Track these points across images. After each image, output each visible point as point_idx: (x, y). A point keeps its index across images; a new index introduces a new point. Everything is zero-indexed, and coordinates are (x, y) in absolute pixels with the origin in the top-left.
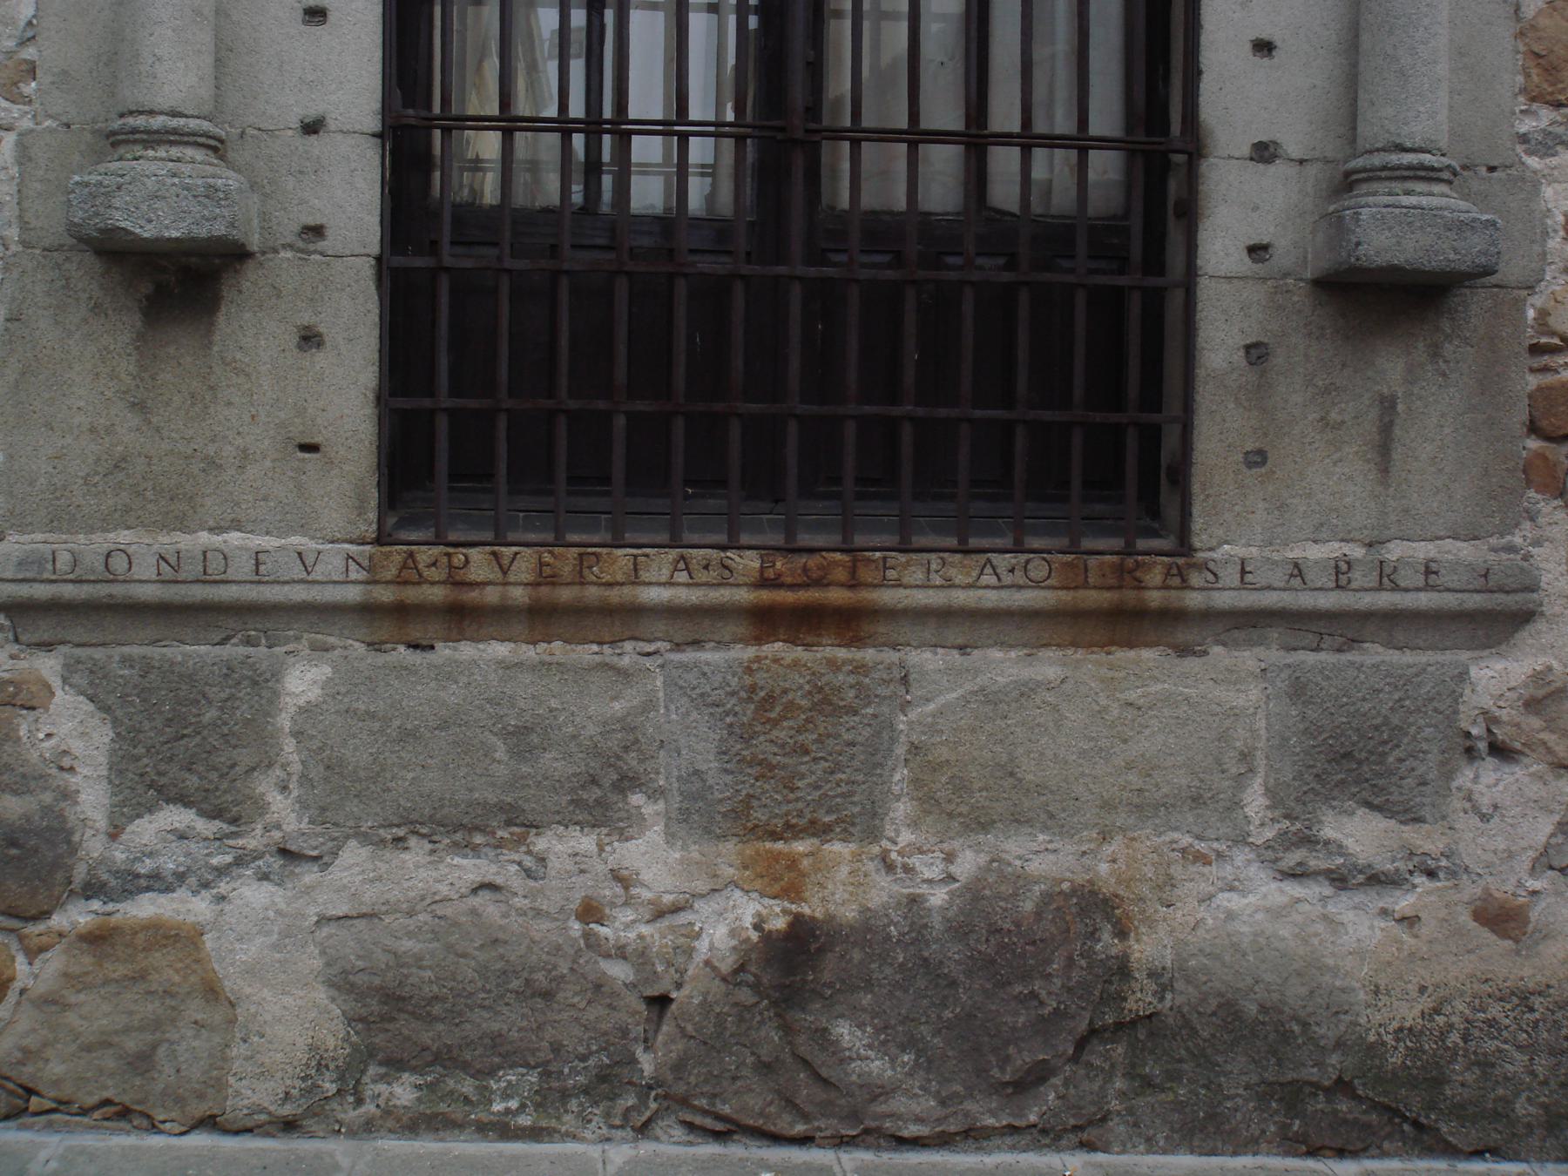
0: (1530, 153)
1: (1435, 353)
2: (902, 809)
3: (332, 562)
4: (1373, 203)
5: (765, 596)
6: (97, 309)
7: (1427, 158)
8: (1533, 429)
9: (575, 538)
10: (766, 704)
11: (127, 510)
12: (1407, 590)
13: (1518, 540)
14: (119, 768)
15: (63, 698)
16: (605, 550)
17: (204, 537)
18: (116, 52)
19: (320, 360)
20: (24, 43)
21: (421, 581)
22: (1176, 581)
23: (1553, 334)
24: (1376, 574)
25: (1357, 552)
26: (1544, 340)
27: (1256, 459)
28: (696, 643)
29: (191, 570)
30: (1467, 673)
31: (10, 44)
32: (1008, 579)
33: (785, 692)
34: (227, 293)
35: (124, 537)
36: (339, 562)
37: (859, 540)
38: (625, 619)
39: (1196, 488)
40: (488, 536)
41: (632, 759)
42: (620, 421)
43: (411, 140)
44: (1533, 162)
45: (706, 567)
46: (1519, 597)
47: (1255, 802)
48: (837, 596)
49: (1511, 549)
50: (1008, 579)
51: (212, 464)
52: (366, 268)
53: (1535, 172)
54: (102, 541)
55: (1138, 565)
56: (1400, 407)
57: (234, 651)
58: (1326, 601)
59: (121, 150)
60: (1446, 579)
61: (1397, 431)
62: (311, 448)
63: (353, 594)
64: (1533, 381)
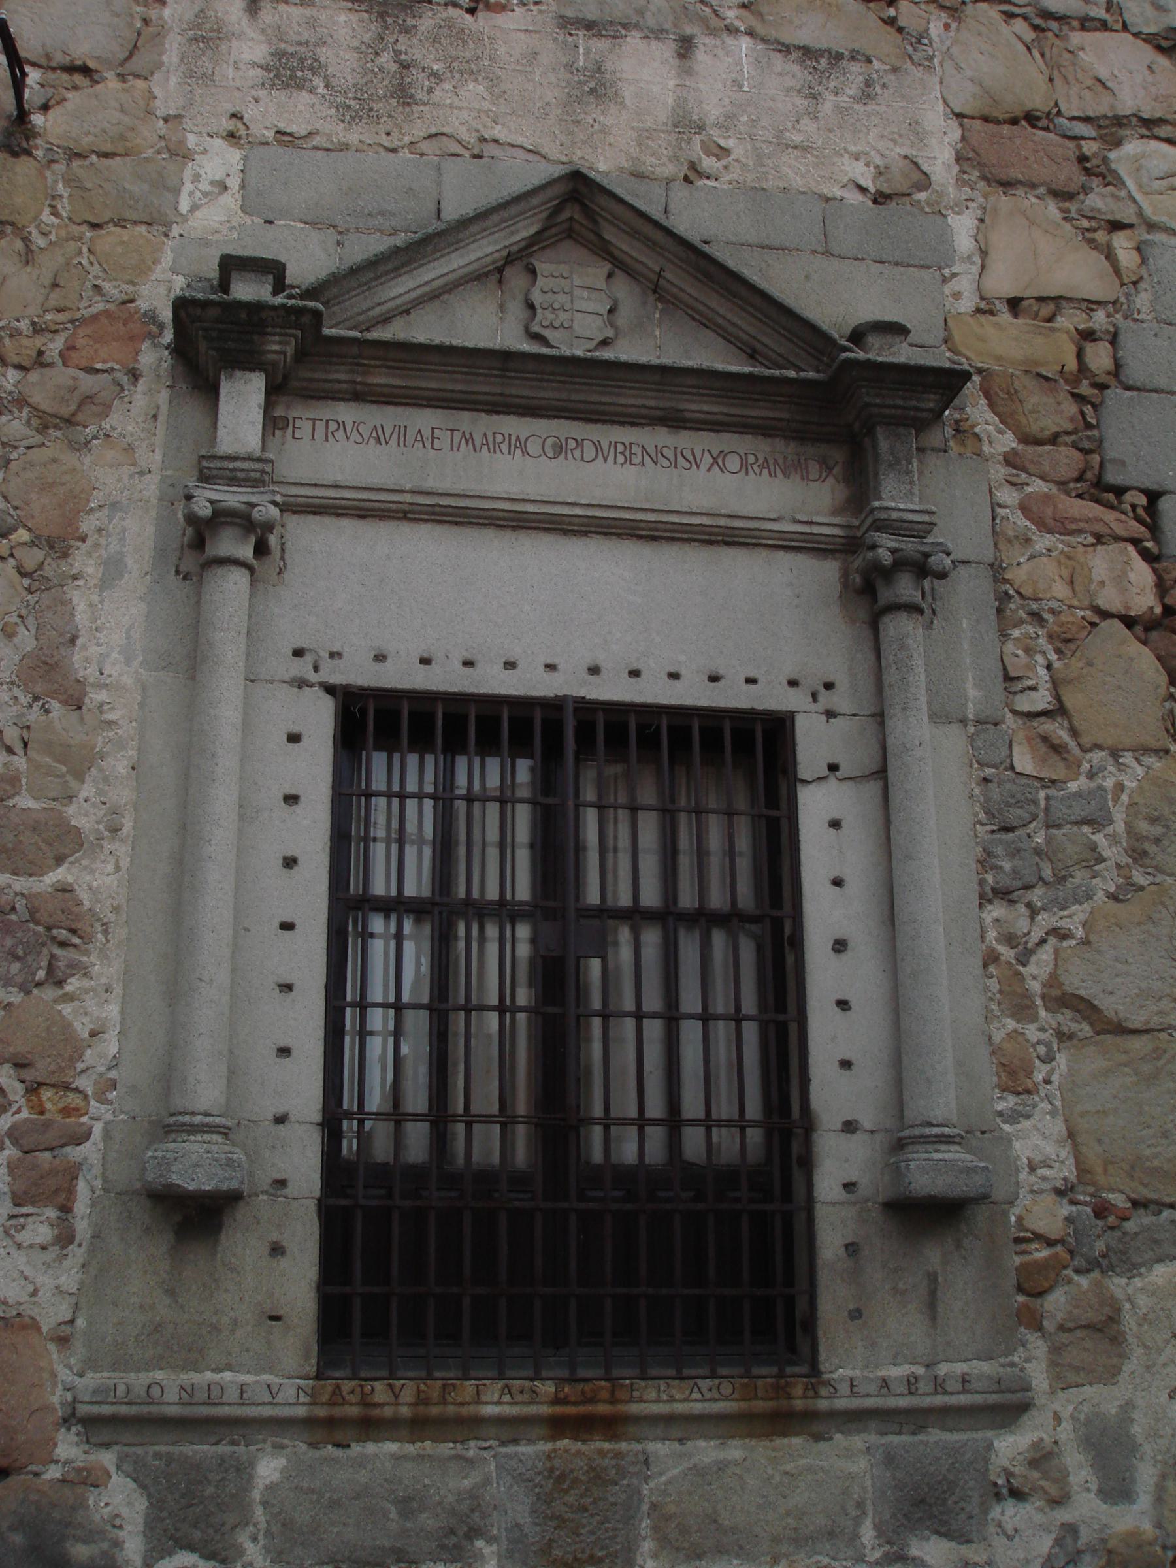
0: (1004, 1122)
1: (959, 1245)
2: (647, 1546)
3: (289, 1392)
5: (559, 1409)
6: (147, 1230)
7: (946, 1130)
8: (1020, 1289)
10: (560, 1479)
12: (952, 1393)
13: (1016, 1359)
14: (152, 1525)
15: (117, 1479)
16: (458, 1382)
17: (209, 1375)
18: (169, 1074)
19: (284, 1263)
20: (109, 1069)
21: (344, 1402)
22: (811, 1393)
23: (1027, 1230)
24: (932, 1384)
25: (920, 1371)
26: (1022, 1235)
27: (856, 1314)
28: (515, 1441)
29: (201, 1396)
30: (992, 1444)
31: (103, 1069)
32: (708, 1395)
33: (572, 1471)
35: (159, 1375)
36: (293, 1391)
37: (616, 1373)
38: (469, 1426)
39: (820, 1333)
40: (385, 1373)
41: (476, 1516)
42: (467, 1302)
44: (1007, 1127)
45: (522, 1392)
46: (1019, 1395)
47: (868, 1534)
48: (602, 1409)
49: (1012, 1365)
50: (708, 1395)
51: (215, 1329)
52: (312, 1205)
53: (1008, 1133)
54: (145, 1378)
55: (787, 1382)
56: (940, 1279)
57: (224, 1449)
58: (903, 1402)
59: (174, 1136)
60: (975, 1385)
61: (939, 1294)
62: (276, 1318)
63: (301, 1412)
64: (1017, 1260)
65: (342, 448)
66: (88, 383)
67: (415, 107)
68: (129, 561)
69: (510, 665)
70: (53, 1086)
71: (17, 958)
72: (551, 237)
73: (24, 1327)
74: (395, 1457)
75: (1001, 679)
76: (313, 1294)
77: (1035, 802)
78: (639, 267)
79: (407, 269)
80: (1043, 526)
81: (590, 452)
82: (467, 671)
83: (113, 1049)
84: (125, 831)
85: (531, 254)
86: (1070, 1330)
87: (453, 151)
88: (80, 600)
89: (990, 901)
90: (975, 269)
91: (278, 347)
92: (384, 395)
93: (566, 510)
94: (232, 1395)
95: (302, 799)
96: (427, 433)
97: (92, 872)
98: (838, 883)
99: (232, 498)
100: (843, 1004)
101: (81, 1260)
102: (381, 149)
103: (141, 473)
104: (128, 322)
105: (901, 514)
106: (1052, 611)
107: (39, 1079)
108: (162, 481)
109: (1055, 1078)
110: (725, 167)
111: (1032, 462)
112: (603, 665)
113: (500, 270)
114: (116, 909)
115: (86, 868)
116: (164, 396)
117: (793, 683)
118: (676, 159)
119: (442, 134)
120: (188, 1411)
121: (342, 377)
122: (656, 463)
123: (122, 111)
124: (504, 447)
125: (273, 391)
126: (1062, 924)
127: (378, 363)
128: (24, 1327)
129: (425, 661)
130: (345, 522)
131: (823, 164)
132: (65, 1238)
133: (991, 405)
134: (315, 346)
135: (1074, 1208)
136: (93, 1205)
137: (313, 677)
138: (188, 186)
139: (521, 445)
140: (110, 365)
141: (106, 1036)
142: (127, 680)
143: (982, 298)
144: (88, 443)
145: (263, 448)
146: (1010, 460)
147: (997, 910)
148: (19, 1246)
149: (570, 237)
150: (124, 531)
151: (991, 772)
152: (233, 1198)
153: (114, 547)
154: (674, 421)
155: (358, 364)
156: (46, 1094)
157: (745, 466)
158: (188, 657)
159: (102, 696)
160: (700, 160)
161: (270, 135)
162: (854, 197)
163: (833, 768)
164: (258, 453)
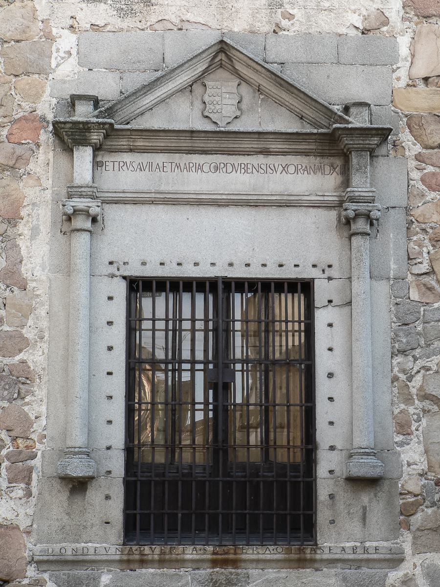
3: (113, 550)
4: (356, 459)
5: (214, 557)
6: (59, 491)
7: (367, 450)
8: (402, 514)
9: (169, 543)
11: (65, 538)
12: (371, 554)
13: (398, 541)
17: (83, 544)
19: (110, 502)
20: (43, 431)
21: (133, 554)
22: (314, 552)
23: (405, 490)
24: (363, 550)
25: (358, 544)
26: (403, 492)
27: (332, 522)
28: (198, 569)
29: (80, 552)
30: (387, 574)
31: (41, 431)
32: (272, 552)
33: (219, 580)
34: (89, 487)
35: (64, 544)
36: (114, 550)
37: (237, 543)
38: (180, 563)
39: (318, 529)
40: (149, 543)
42: (180, 515)
43: (129, 451)
44: (398, 449)
45: (200, 550)
46: (399, 555)
48: (231, 556)
49: (397, 543)
50: (272, 552)
51: (85, 527)
54: (59, 546)
56: (367, 509)
58: (351, 557)
60: (380, 551)
61: (367, 514)
63: (117, 558)
64: (401, 502)
65: (126, 173)
66: (19, 150)
67: (152, 8)
68: (41, 228)
69: (196, 264)
70: (22, 438)
71: (7, 390)
72: (211, 69)
73: (14, 528)
74: (153, 574)
75: (407, 259)
76: (121, 514)
77: (419, 312)
78: (251, 80)
79: (150, 92)
80: (431, 188)
81: (230, 169)
82: (180, 267)
83: (44, 423)
84: (46, 338)
85: (204, 77)
86: (422, 530)
87: (169, 28)
88: (22, 244)
89: (397, 355)
90: (408, 64)
91: (96, 137)
92: (142, 150)
93: (219, 197)
94: (92, 551)
95: (114, 323)
96: (161, 165)
97: (34, 355)
98: (330, 349)
99: (81, 203)
100: (331, 399)
101: (35, 503)
102: (138, 29)
103: (44, 190)
104: (34, 120)
105: (359, 193)
106: (432, 228)
107: (17, 436)
108: (53, 192)
109: (420, 428)
110: (292, 24)
111: (428, 158)
112: (235, 262)
113: (191, 86)
114: (44, 369)
115: (31, 353)
116: (51, 154)
117: (314, 266)
118: (270, 22)
119: (165, 20)
120: (74, 558)
121: (125, 143)
122: (258, 172)
123: (23, 18)
124: (194, 169)
125: (97, 149)
126: (427, 364)
127: (139, 137)
128: (14, 528)
129: (162, 264)
130: (128, 206)
131: (338, 17)
132: (29, 494)
133: (411, 132)
134: (110, 132)
135: (426, 481)
136: (39, 482)
137: (117, 273)
138: (54, 55)
139: (200, 168)
140: (28, 141)
141: (41, 418)
142: (44, 278)
143: (410, 79)
144: (21, 177)
145: (93, 182)
146: (418, 158)
147: (399, 359)
148: (11, 498)
149: (221, 67)
150: (39, 215)
151: (399, 302)
152: (92, 478)
153: (35, 222)
154: (266, 152)
155: (131, 138)
156: (20, 441)
157: (297, 170)
158: (66, 269)
159: (34, 284)
160: (280, 22)
161: (88, 26)
162: (353, 33)
163: (330, 301)
164: (91, 184)
